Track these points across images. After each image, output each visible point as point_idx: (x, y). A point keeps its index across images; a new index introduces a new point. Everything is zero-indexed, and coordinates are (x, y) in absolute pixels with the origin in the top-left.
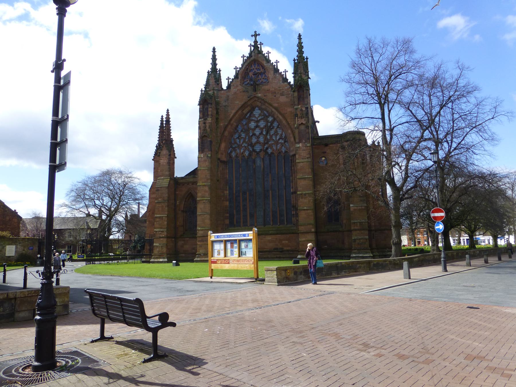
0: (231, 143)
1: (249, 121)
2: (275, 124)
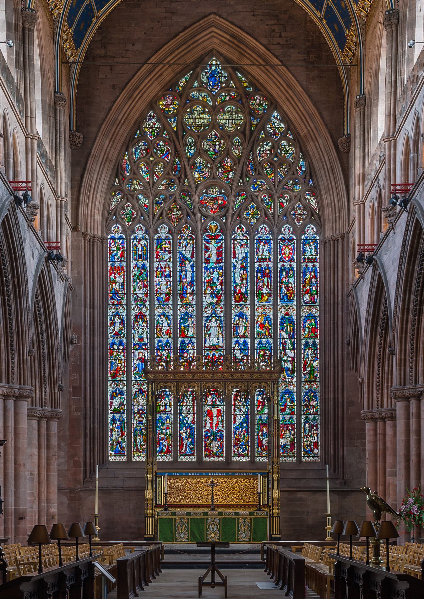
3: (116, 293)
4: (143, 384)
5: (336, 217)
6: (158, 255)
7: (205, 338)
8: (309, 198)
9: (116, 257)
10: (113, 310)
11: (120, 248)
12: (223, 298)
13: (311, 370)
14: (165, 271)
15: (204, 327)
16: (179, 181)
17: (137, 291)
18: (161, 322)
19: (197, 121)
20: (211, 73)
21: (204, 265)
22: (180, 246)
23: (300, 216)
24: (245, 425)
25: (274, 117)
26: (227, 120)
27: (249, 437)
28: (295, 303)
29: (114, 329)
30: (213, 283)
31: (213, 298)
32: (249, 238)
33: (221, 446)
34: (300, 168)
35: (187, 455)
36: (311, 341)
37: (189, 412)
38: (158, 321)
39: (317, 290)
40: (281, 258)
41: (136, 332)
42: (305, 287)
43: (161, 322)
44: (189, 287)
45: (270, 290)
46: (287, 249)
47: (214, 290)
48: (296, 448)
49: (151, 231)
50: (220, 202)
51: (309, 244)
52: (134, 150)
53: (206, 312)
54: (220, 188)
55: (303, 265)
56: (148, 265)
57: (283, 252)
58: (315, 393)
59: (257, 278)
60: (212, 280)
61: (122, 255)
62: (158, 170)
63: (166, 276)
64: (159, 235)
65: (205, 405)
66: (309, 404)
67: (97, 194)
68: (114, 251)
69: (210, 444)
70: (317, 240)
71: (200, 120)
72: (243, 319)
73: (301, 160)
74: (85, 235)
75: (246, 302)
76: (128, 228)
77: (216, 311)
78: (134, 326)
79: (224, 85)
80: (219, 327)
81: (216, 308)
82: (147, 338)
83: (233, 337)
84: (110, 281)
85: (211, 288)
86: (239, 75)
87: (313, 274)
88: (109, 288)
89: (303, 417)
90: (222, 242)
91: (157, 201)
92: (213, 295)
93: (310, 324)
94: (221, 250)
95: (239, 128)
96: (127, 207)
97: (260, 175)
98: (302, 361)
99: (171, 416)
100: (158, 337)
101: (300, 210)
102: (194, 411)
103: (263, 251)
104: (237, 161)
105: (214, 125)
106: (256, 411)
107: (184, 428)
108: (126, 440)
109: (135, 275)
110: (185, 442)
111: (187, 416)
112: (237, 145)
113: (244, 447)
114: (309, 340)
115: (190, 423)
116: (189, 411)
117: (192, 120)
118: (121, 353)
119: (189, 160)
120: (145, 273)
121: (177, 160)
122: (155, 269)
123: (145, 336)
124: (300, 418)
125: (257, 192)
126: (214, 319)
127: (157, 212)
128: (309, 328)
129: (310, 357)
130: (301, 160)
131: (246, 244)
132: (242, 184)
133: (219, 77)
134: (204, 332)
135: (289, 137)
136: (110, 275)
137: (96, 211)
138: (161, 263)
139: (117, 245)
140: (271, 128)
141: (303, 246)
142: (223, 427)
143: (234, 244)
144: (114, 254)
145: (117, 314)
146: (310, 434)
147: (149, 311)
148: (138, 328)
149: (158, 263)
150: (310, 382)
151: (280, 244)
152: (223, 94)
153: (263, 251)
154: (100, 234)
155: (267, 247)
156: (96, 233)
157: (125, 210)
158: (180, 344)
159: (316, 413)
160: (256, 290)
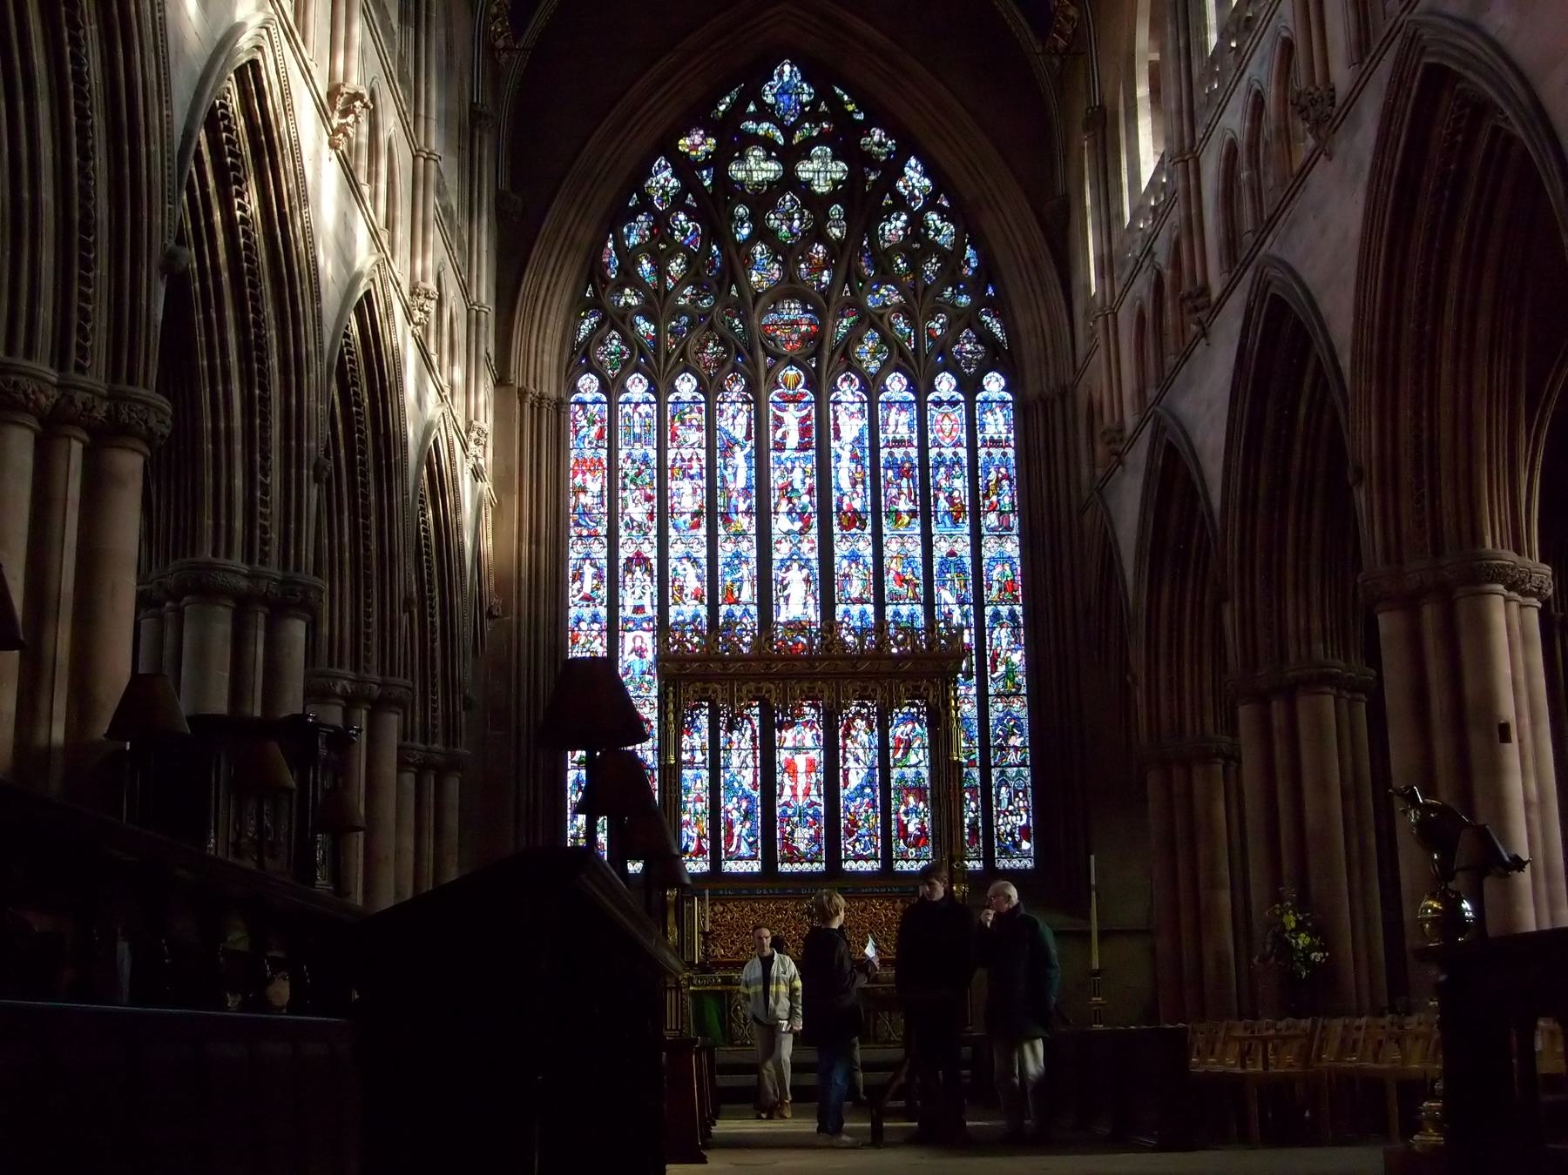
0: (593, 271)
1: (733, 143)
2: (914, 179)
3: (586, 513)
4: (644, 704)
5: (1046, 357)
6: (676, 435)
7: (778, 605)
8: (989, 321)
9: (587, 440)
10: (579, 548)
11: (594, 423)
12: (814, 521)
13: (1008, 671)
14: (691, 468)
15: (774, 582)
16: (720, 289)
17: (631, 509)
18: (684, 573)
19: (755, 174)
20: (781, 87)
21: (773, 454)
22: (721, 416)
23: (970, 356)
24: (868, 790)
25: (910, 167)
26: (814, 172)
27: (877, 817)
28: (967, 530)
29: (582, 587)
30: (793, 490)
31: (793, 521)
32: (866, 399)
33: (814, 839)
34: (967, 262)
35: (741, 858)
36: (1004, 610)
37: (744, 765)
38: (675, 570)
39: (1013, 503)
40: (935, 440)
41: (630, 592)
42: (986, 496)
43: (684, 573)
44: (741, 499)
45: (914, 502)
46: (946, 421)
47: (794, 505)
48: (981, 841)
49: (660, 387)
50: (804, 328)
51: (992, 411)
52: (625, 230)
53: (778, 550)
54: (804, 304)
55: (982, 452)
56: (653, 454)
57: (938, 427)
58: (1018, 719)
59: (886, 480)
60: (791, 484)
61: (600, 436)
62: (676, 266)
63: (692, 477)
64: (676, 394)
65: (780, 748)
66: (1006, 742)
67: (549, 313)
68: (582, 427)
69: (793, 832)
70: (1008, 402)
71: (760, 173)
72: (857, 564)
73: (968, 247)
74: (522, 393)
75: (863, 530)
76: (614, 380)
77: (799, 549)
78: (624, 582)
79: (807, 109)
80: (807, 581)
81: (800, 541)
82: (652, 606)
83: (837, 601)
84: (574, 487)
85: (790, 500)
86: (838, 91)
87: (1003, 470)
88: (572, 502)
89: (995, 772)
90: (809, 408)
91: (672, 327)
92: (794, 515)
93: (1003, 574)
94: (808, 423)
95: (840, 187)
96: (610, 340)
97: (885, 275)
98: (988, 652)
99: (705, 774)
100: (676, 603)
101: (969, 342)
102: (755, 762)
103: (897, 425)
104: (834, 247)
105: (789, 181)
106: (892, 760)
107: (735, 800)
108: (606, 827)
109: (626, 475)
110: (737, 830)
111: (739, 773)
112: (837, 220)
113: (867, 838)
114: (1000, 608)
115: (746, 787)
116: (744, 762)
117: (744, 173)
118: (595, 638)
119: (739, 245)
120: (649, 471)
121: (714, 247)
122: (670, 463)
123: (646, 601)
124: (990, 775)
125: (880, 308)
126: (795, 566)
127: (674, 350)
128: (1000, 582)
129: (1004, 646)
130: (968, 247)
131: (861, 411)
132: (849, 294)
133: (798, 94)
134: (774, 593)
135: (941, 205)
136: (574, 477)
137: (547, 347)
138: (682, 450)
139: (589, 415)
140: (905, 187)
141: (981, 414)
142: (819, 795)
143: (835, 412)
144: (582, 433)
145: (588, 557)
146: (1011, 808)
147: (655, 550)
148: (633, 585)
149: (676, 450)
150: (1008, 697)
151: (933, 413)
152: (807, 125)
153: (897, 425)
154: (553, 394)
155: (904, 417)
156: (545, 390)
157: (605, 345)
158: (724, 617)
159: (1023, 764)
160: (883, 503)
